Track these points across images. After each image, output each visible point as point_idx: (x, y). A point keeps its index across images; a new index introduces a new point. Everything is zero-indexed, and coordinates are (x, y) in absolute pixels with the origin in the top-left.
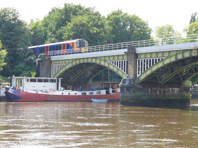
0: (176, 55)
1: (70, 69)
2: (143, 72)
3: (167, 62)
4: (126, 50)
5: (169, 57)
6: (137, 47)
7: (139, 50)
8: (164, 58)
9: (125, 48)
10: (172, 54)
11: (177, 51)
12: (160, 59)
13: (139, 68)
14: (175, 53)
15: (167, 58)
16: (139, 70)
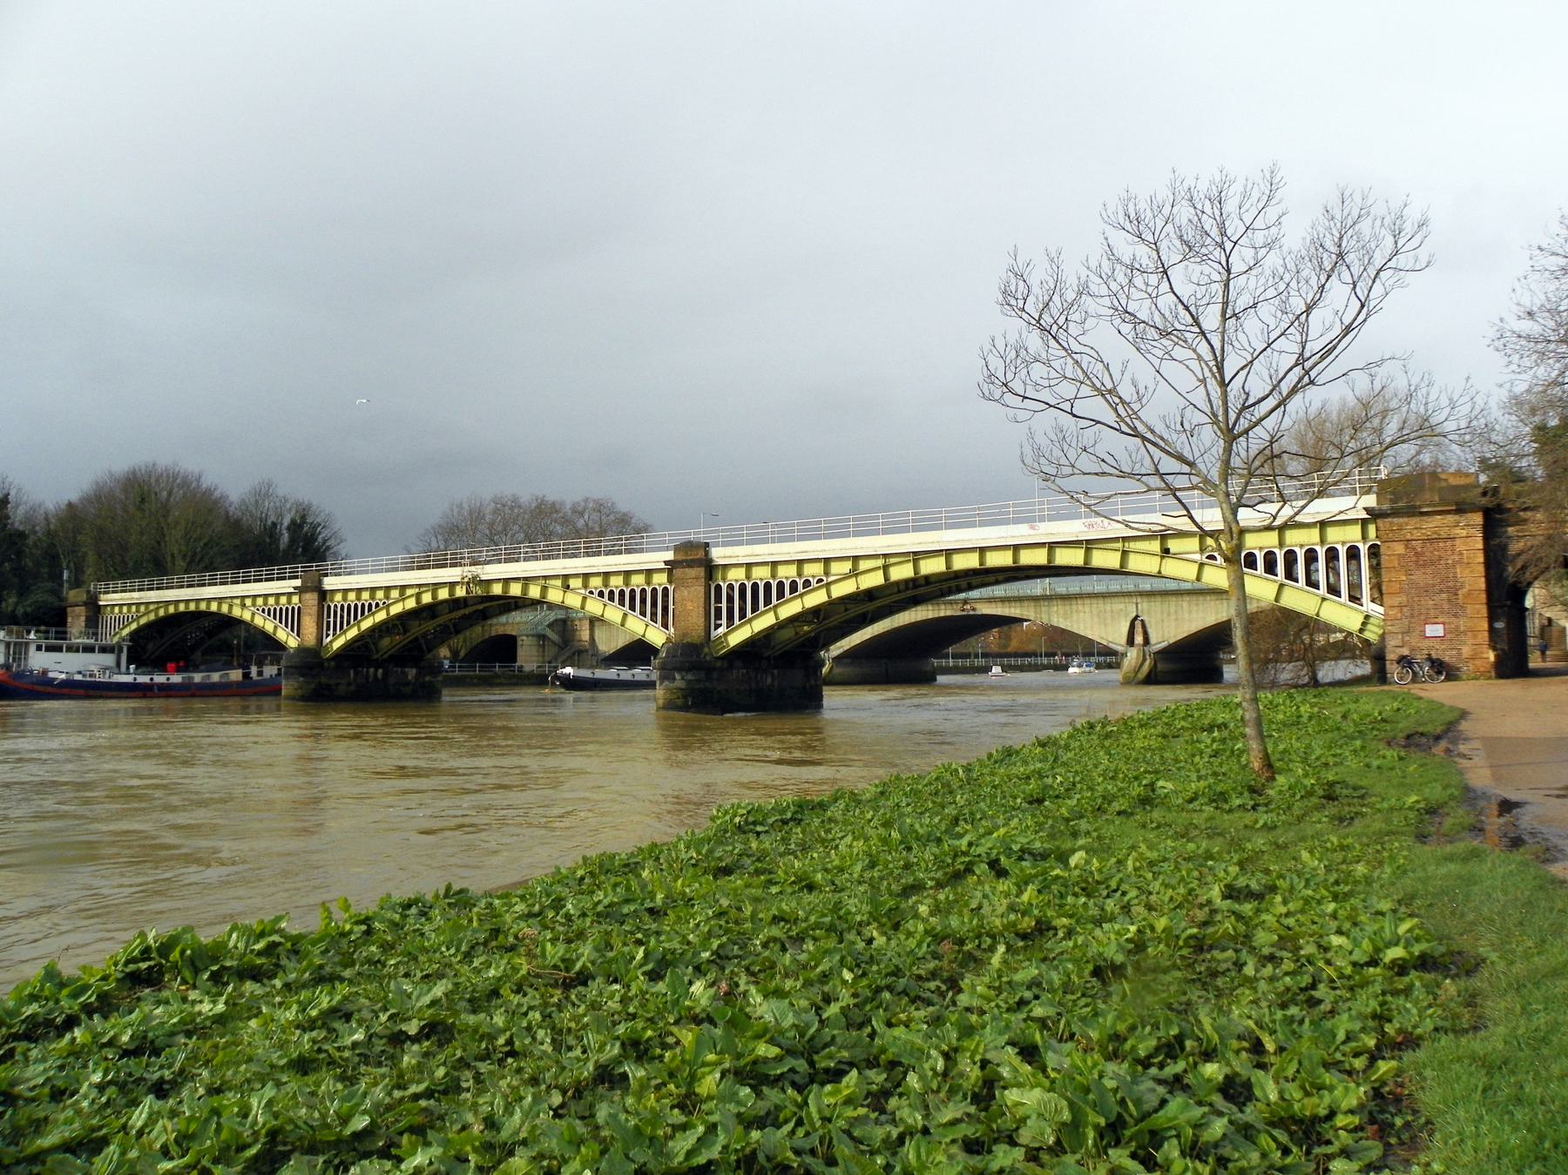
0: (886, 568)
1: (149, 625)
2: (737, 622)
3: (839, 590)
4: (298, 583)
5: (854, 573)
6: (326, 575)
7: (329, 583)
8: (832, 579)
9: (296, 577)
10: (863, 565)
11: (885, 556)
12: (813, 582)
13: (719, 610)
14: (880, 562)
15: (846, 577)
16: (718, 616)
